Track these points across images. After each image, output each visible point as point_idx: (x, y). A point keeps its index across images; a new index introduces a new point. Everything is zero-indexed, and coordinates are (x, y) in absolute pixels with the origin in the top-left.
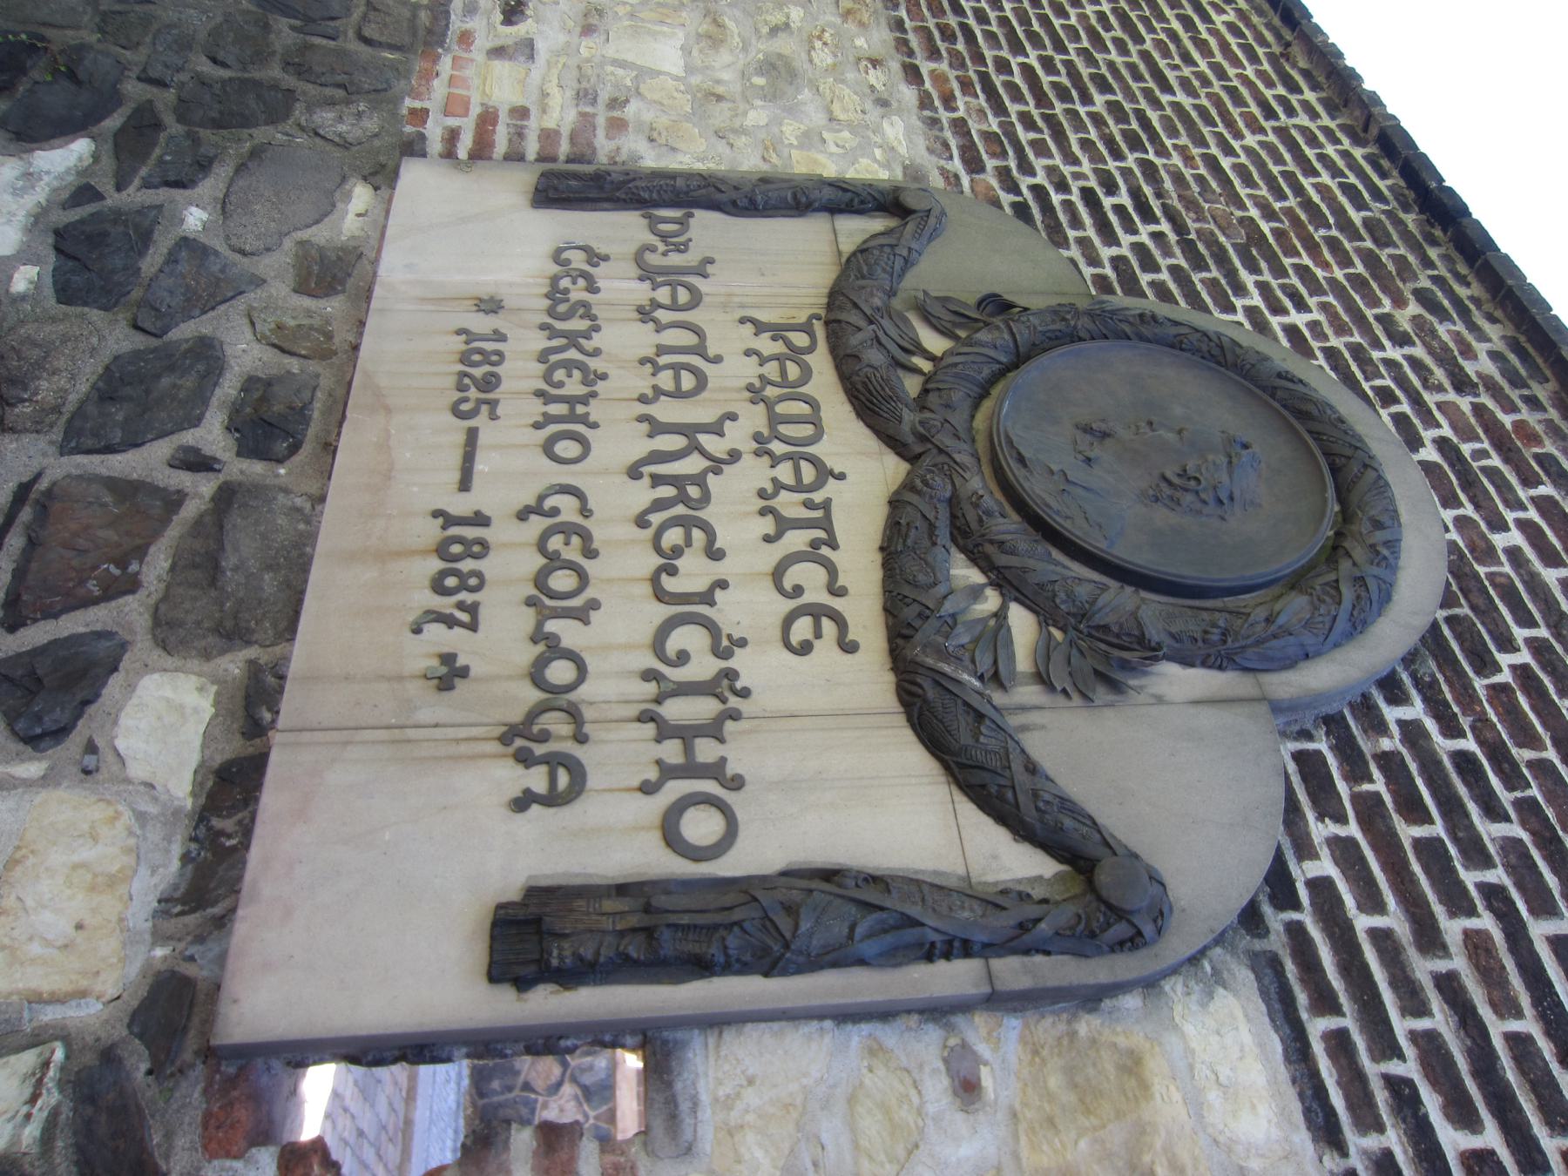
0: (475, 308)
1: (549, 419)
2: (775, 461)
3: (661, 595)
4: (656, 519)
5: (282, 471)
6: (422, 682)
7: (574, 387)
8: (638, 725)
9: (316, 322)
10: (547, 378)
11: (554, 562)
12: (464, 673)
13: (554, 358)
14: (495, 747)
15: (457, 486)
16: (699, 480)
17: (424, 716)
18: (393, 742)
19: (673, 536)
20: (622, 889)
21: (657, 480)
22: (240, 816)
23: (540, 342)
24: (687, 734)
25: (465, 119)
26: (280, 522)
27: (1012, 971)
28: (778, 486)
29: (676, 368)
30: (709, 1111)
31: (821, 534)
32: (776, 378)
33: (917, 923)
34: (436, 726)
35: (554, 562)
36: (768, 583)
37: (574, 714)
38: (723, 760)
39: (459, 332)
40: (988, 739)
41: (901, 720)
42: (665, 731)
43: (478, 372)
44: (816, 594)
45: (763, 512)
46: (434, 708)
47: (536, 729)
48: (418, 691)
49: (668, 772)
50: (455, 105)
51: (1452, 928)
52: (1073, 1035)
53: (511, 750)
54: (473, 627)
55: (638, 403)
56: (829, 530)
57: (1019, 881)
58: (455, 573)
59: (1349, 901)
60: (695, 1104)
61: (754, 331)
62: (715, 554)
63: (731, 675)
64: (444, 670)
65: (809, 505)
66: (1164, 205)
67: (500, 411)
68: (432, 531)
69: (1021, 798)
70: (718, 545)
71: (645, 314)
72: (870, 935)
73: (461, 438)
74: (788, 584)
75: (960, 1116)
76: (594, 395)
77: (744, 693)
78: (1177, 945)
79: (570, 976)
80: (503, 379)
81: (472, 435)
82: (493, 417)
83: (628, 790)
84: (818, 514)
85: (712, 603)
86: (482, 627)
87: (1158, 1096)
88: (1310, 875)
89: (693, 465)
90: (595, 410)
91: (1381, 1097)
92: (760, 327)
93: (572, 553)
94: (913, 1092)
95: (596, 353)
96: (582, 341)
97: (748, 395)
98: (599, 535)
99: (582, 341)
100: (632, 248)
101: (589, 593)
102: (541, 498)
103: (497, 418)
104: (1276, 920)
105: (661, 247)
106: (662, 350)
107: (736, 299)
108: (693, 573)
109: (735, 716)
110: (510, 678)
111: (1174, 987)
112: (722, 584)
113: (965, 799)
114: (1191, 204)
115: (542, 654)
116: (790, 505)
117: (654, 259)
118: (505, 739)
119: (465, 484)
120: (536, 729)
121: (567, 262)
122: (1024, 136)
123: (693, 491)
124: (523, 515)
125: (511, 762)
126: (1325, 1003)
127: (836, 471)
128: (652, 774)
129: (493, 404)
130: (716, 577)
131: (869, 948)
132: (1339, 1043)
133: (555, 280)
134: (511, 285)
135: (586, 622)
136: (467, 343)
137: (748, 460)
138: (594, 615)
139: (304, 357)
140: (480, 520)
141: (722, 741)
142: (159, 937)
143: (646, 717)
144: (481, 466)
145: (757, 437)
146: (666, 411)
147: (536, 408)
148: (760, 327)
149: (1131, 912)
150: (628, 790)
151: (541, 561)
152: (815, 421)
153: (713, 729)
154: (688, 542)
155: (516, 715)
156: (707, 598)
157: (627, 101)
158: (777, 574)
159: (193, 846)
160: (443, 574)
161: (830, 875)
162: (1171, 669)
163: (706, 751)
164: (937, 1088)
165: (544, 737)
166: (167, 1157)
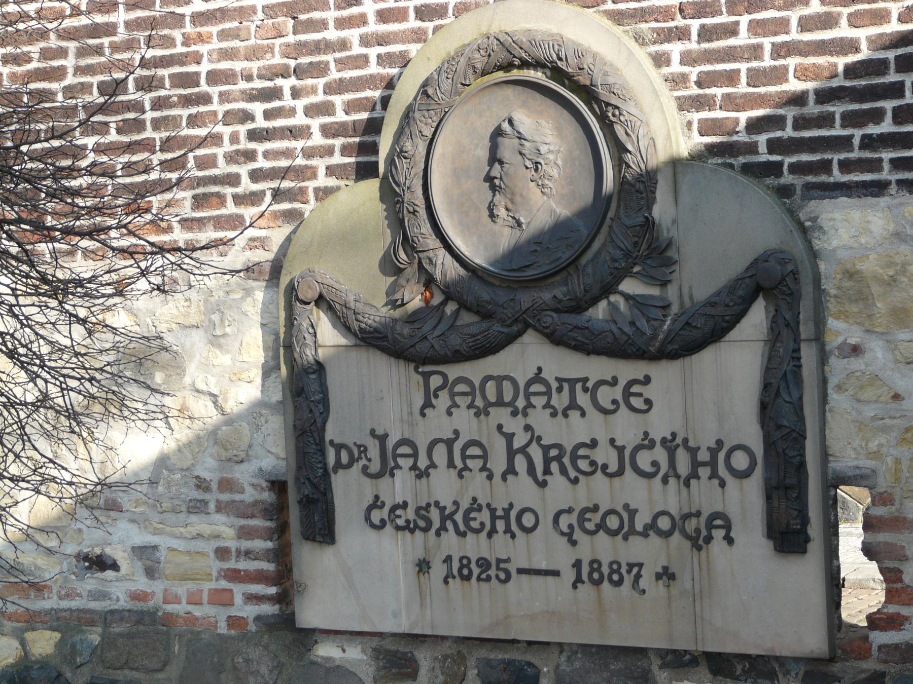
0: (426, 574)
1: (508, 530)
2: (530, 405)
3: (620, 472)
4: (573, 474)
5: (545, 669)
6: (671, 588)
7: (485, 516)
8: (691, 487)
9: (437, 665)
10: (477, 531)
11: (601, 526)
12: (665, 569)
13: (462, 528)
14: (703, 553)
15: (557, 577)
16: (546, 449)
17: (688, 585)
18: (701, 598)
19: (583, 465)
20: (769, 498)
21: (547, 471)
22: (735, 663)
23: (450, 536)
24: (696, 464)
25: (235, 591)
26: (578, 666)
27: (806, 330)
28: (547, 405)
29: (464, 457)
30: (860, 462)
31: (579, 386)
32: (469, 399)
33: (785, 374)
34: (693, 579)
35: (601, 526)
36: (611, 417)
37: (686, 517)
38: (709, 449)
39: (446, 582)
40: (699, 323)
41: (687, 360)
42: (694, 475)
43: (476, 571)
44: (617, 393)
45: (566, 415)
46: (685, 581)
47: (694, 535)
49: (714, 475)
50: (221, 598)
52: (836, 296)
53: (704, 546)
54: (640, 565)
55: (493, 481)
56: (578, 380)
57: (767, 317)
59: (778, 134)
60: (858, 467)
61: (431, 409)
62: (594, 444)
63: (664, 441)
64: (665, 578)
65: (560, 390)
66: (260, 77)
67: (505, 557)
68: (586, 589)
69: (729, 313)
70: (588, 442)
71: (422, 474)
72: (790, 394)
73: (524, 578)
74: (612, 407)
75: (866, 355)
76: (488, 505)
77: (674, 435)
78: (797, 248)
79: (805, 521)
80: (480, 556)
81: (521, 571)
82: (507, 561)
83: (723, 492)
84: (566, 386)
85: (624, 447)
86: (641, 561)
87: (861, 267)
88: (766, 151)
89: (536, 453)
90: (500, 505)
91: (867, 155)
92: (428, 404)
93: (597, 518)
95: (456, 503)
96: (447, 512)
97: (482, 417)
98: (584, 504)
99: (447, 512)
100: (367, 481)
101: (620, 509)
102: (563, 534)
103: (509, 558)
104: (787, 178)
105: (363, 462)
106: (451, 464)
107: (405, 417)
108: (605, 455)
109: (686, 441)
110: (668, 546)
111: (817, 244)
112: (612, 441)
113: (728, 335)
114: (253, 54)
115: (654, 531)
116: (560, 401)
117: (375, 467)
118: (699, 549)
119: (556, 573)
120: (694, 535)
121: (383, 523)
123: (554, 453)
124: (574, 543)
126: (825, 166)
127: (536, 371)
128: (716, 482)
129: (499, 561)
130: (608, 444)
131: (795, 394)
132: (845, 166)
133: (398, 528)
134: (405, 554)
135: (636, 511)
136: (454, 577)
138: (632, 507)
139: (465, 669)
140: (577, 564)
141: (699, 448)
143: (687, 484)
144: (543, 566)
145: (514, 414)
146: (498, 463)
147: (501, 538)
148: (428, 404)
149: (782, 274)
150: (723, 492)
151: (601, 533)
152: (499, 380)
153: (693, 452)
154: (586, 457)
155: (688, 544)
156: (621, 450)
157: (197, 477)
158: (605, 412)
159: (749, 680)
160: (611, 581)
161: (764, 407)
162: (657, 212)
163: (704, 456)
164: (856, 364)
165: (698, 531)
166: (870, 670)
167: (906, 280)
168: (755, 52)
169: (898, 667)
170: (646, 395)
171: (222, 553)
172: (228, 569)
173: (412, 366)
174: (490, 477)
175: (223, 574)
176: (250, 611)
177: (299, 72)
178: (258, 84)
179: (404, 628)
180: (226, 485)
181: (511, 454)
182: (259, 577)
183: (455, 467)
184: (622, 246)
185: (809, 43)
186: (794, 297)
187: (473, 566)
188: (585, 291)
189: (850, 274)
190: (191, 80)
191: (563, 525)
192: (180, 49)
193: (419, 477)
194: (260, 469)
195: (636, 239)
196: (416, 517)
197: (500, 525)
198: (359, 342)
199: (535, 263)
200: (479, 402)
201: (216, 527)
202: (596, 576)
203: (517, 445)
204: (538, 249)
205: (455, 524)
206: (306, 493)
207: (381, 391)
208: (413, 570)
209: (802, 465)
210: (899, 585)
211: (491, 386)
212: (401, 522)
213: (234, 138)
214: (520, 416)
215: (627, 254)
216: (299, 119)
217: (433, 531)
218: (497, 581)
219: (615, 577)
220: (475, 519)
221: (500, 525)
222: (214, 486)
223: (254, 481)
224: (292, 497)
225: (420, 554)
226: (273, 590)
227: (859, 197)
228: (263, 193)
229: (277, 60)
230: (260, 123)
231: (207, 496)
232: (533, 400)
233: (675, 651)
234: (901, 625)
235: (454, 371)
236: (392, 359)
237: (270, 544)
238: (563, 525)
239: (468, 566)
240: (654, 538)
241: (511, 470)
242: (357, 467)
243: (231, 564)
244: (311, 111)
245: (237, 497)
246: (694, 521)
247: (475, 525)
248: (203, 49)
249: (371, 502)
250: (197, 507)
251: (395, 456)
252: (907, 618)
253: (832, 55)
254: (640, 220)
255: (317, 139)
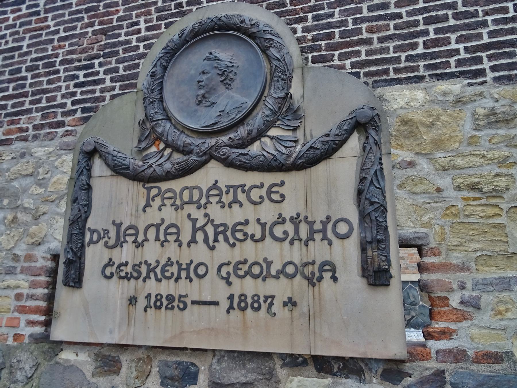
0: (134, 306)
3: (262, 239)
4: (232, 241)
5: (203, 368)
6: (293, 311)
7: (174, 269)
8: (309, 246)
9: (133, 365)
10: (169, 278)
11: (248, 273)
12: (290, 299)
13: (159, 276)
14: (316, 288)
15: (217, 306)
16: (216, 227)
17: (305, 309)
20: (363, 250)
21: (216, 240)
22: (333, 363)
24: (313, 232)
25: (21, 318)
26: (225, 366)
29: (166, 234)
31: (239, 190)
33: (376, 172)
35: (248, 273)
36: (258, 207)
37: (306, 264)
38: (321, 222)
39: (145, 310)
40: (318, 145)
41: (308, 170)
43: (165, 303)
44: (263, 192)
45: (230, 206)
46: (302, 306)
47: (310, 276)
48: (296, 312)
50: (13, 324)
51: (365, 35)
52: (395, 136)
53: (317, 283)
54: (273, 297)
55: (182, 247)
56: (239, 186)
57: (359, 143)
58: (252, 304)
59: (357, 59)
60: (416, 232)
61: (149, 207)
63: (292, 219)
64: (289, 305)
65: (227, 193)
66: (84, 60)
67: (184, 294)
68: (236, 314)
69: (338, 139)
70: (243, 221)
71: (138, 245)
72: (379, 183)
73: (196, 307)
75: (417, 167)
76: (177, 262)
77: (298, 215)
80: (169, 293)
81: (193, 303)
82: (186, 296)
83: (331, 248)
84: (232, 190)
85: (266, 223)
86: (273, 294)
87: (413, 117)
89: (210, 230)
90: (184, 262)
91: (410, 64)
92: (148, 205)
93: (246, 268)
94: (411, 178)
96: (151, 267)
97: (179, 210)
98: (238, 259)
100: (106, 250)
101: (261, 261)
102: (223, 278)
103: (187, 294)
105: (106, 239)
106: (157, 239)
107: (134, 212)
108: (254, 229)
109: (306, 218)
110: (292, 284)
112: (258, 220)
113: (334, 155)
115: (283, 275)
117: (112, 242)
118: (314, 285)
119: (216, 304)
120: (310, 276)
121: (112, 274)
122: (44, 104)
123: (221, 229)
124: (229, 284)
125: (321, 282)
126: (386, 72)
127: (214, 182)
128: (326, 242)
129: (180, 296)
130: (256, 222)
133: (121, 278)
134: (122, 293)
135: (272, 262)
136: (151, 307)
137: (208, 211)
138: (269, 259)
139: (151, 367)
140: (231, 298)
141: (315, 222)
142: (371, 382)
144: (209, 299)
145: (199, 208)
146: (186, 236)
147: (183, 282)
148: (148, 205)
149: (373, 115)
150: (331, 248)
151: (248, 277)
153: (310, 224)
154: (241, 231)
155: (306, 282)
156: (263, 225)
157: (15, 254)
158: (255, 203)
159: (343, 376)
160: (252, 307)
163: (318, 226)
165: (313, 274)
166: (433, 368)
167: (440, 124)
168: (343, 23)
169: (454, 365)
170: (281, 192)
171: (19, 297)
172: (20, 306)
173: (141, 184)
174: (180, 246)
175: (16, 308)
176: (27, 331)
177: (105, 56)
178: (83, 63)
179: (115, 340)
180: (29, 258)
181: (195, 231)
182: (36, 310)
183: (159, 240)
184: (272, 108)
185: (372, 17)
186: (377, 128)
187: (164, 300)
188: (248, 134)
189: (405, 122)
190: (53, 64)
191: (224, 273)
192: (50, 52)
193: (137, 247)
194: (49, 248)
195: (280, 105)
196: (132, 271)
197: (184, 274)
198: (113, 173)
199: (219, 122)
200: (178, 202)
201: (19, 282)
202: (243, 305)
203: (198, 225)
204: (222, 114)
205: (156, 274)
206: (69, 257)
207: (122, 199)
208: (126, 303)
209: (386, 229)
210: (446, 309)
211: (186, 194)
212: (123, 274)
213: (67, 87)
214: (202, 208)
215: (274, 113)
216: (101, 76)
217: (141, 279)
218: (178, 309)
219: (256, 305)
220: (168, 271)
221: (184, 274)
222: (22, 259)
223: (44, 255)
224: (62, 260)
225: (132, 293)
226: (43, 318)
227: (408, 84)
228: (76, 110)
229: (95, 52)
230: (82, 79)
231: (17, 265)
232: (211, 199)
233: (292, 355)
234: (450, 336)
235: (164, 186)
236: (131, 181)
237: (46, 291)
238: (224, 273)
239: (160, 300)
240: (283, 279)
241: (193, 241)
242: (102, 242)
243: (22, 303)
244: (106, 72)
245: (33, 264)
246: (310, 267)
247: (168, 274)
248: (60, 51)
249: (107, 262)
250: (10, 271)
251: (125, 235)
252: (454, 331)
253: (387, 21)
254: (282, 94)
255: (108, 83)
